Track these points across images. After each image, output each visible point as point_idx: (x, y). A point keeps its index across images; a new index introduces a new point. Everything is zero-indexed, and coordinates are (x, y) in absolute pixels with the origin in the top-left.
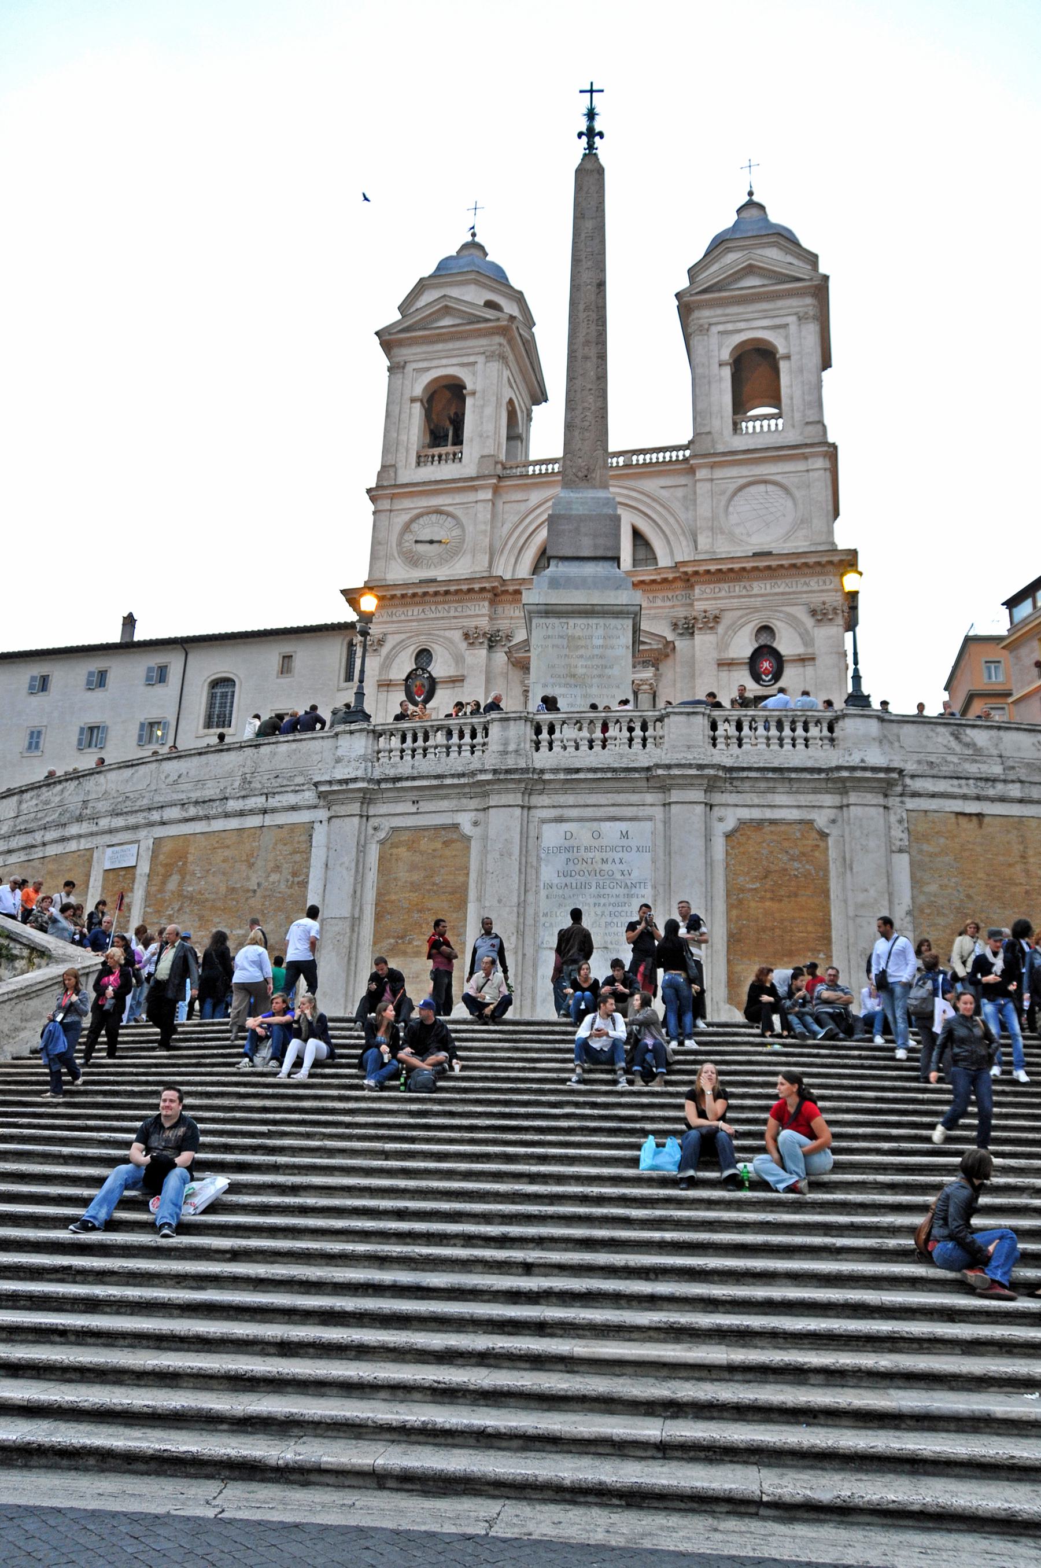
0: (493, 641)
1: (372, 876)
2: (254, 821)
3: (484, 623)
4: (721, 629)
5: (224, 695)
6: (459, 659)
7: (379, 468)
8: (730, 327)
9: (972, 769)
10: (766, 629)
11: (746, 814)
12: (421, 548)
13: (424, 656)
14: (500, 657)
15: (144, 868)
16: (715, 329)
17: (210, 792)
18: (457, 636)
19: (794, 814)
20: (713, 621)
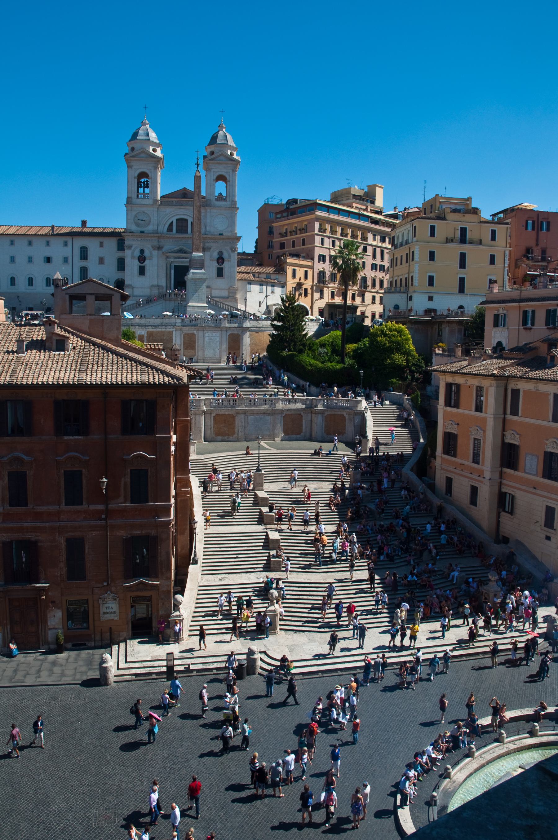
0: (159, 248)
1: (182, 339)
2: (164, 330)
3: (156, 243)
4: (211, 250)
5: (84, 251)
6: (151, 253)
7: (126, 197)
8: (216, 170)
9: (258, 326)
10: (221, 253)
11: (231, 332)
12: (140, 222)
13: (142, 251)
14: (160, 252)
15: (146, 335)
16: (212, 170)
17: (156, 324)
18: (150, 247)
19: (236, 332)
20: (209, 249)
